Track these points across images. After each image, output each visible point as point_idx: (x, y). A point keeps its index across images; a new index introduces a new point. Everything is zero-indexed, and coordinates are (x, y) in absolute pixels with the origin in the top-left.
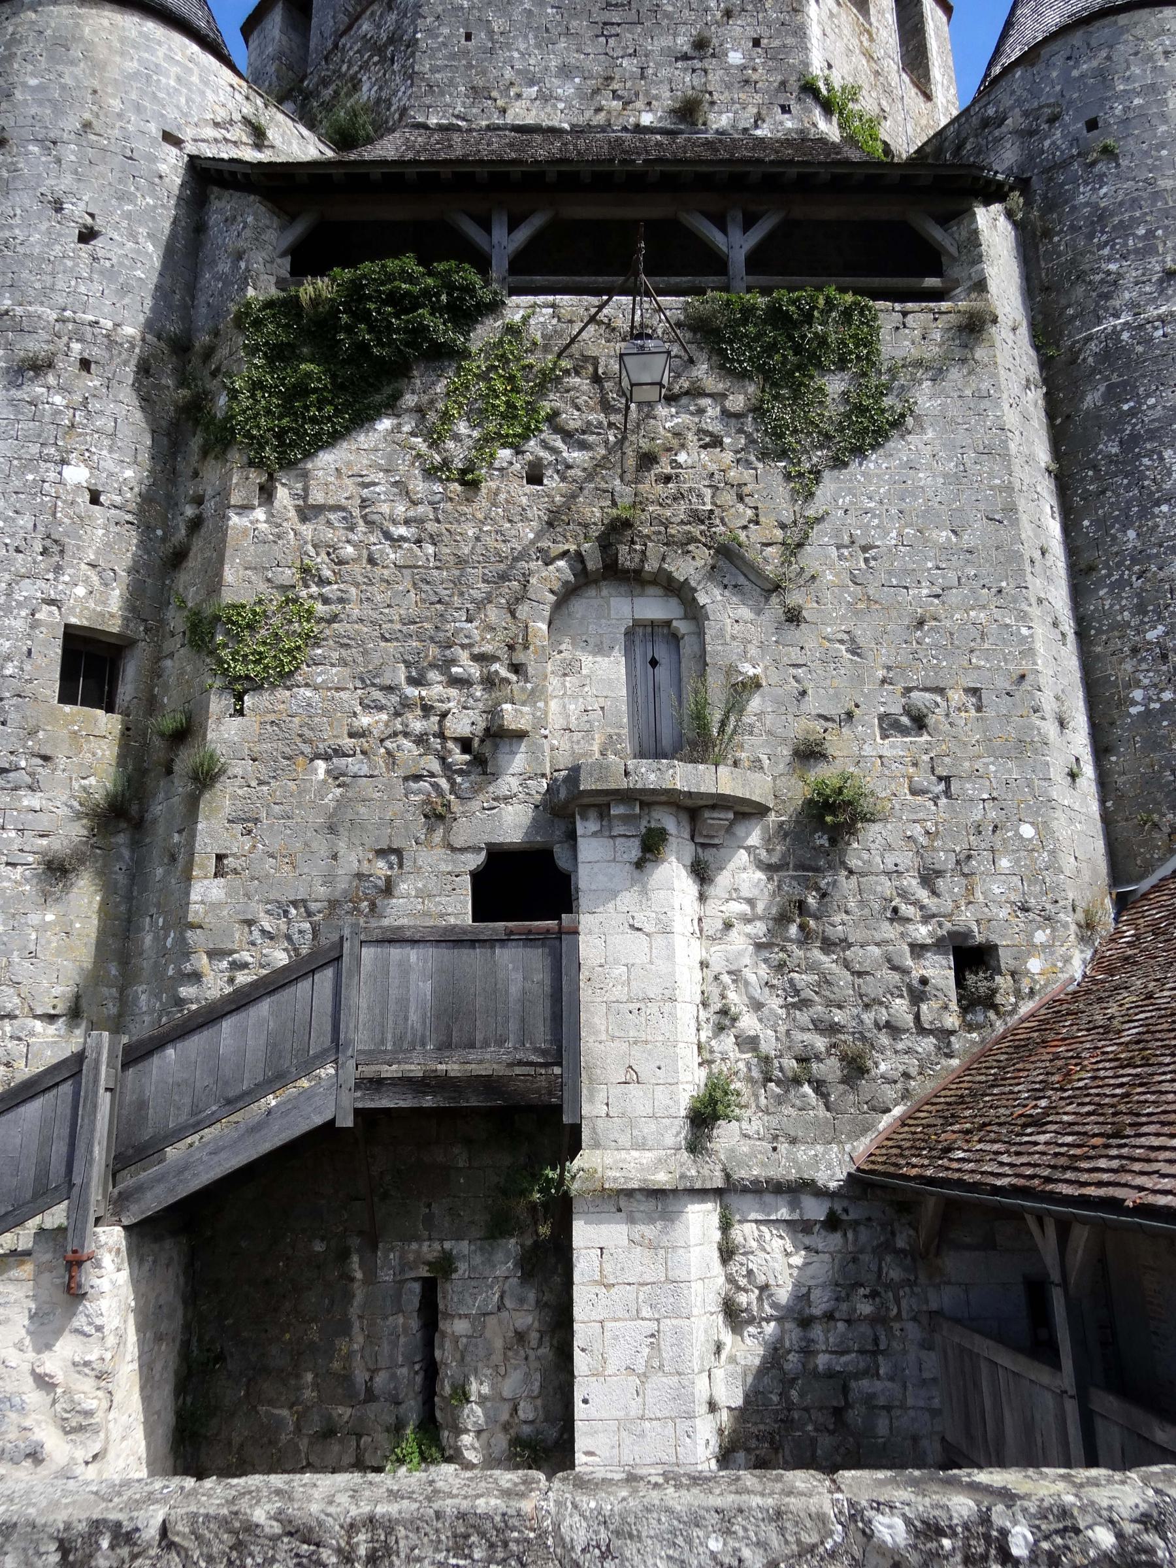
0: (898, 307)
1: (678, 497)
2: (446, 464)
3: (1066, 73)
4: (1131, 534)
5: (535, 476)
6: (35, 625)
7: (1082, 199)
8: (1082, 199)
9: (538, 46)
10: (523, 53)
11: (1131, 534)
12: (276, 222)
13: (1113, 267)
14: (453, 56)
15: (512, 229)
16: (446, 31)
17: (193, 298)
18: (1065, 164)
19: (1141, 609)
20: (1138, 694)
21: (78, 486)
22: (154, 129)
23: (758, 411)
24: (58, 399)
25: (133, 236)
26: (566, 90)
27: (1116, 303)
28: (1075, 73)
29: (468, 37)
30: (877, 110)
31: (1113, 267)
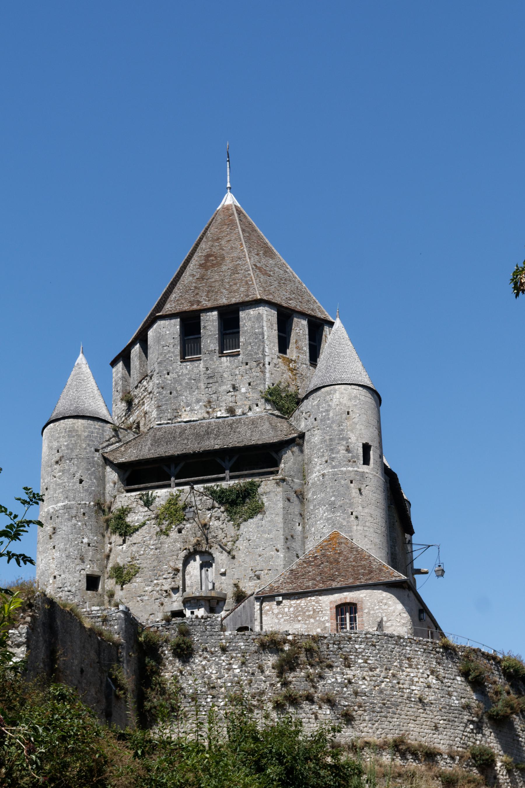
9: (189, 394)
14: (167, 400)
15: (176, 467)
16: (165, 392)
17: (105, 490)
22: (93, 449)
27: (316, 470)
29: (171, 393)
31: (316, 460)
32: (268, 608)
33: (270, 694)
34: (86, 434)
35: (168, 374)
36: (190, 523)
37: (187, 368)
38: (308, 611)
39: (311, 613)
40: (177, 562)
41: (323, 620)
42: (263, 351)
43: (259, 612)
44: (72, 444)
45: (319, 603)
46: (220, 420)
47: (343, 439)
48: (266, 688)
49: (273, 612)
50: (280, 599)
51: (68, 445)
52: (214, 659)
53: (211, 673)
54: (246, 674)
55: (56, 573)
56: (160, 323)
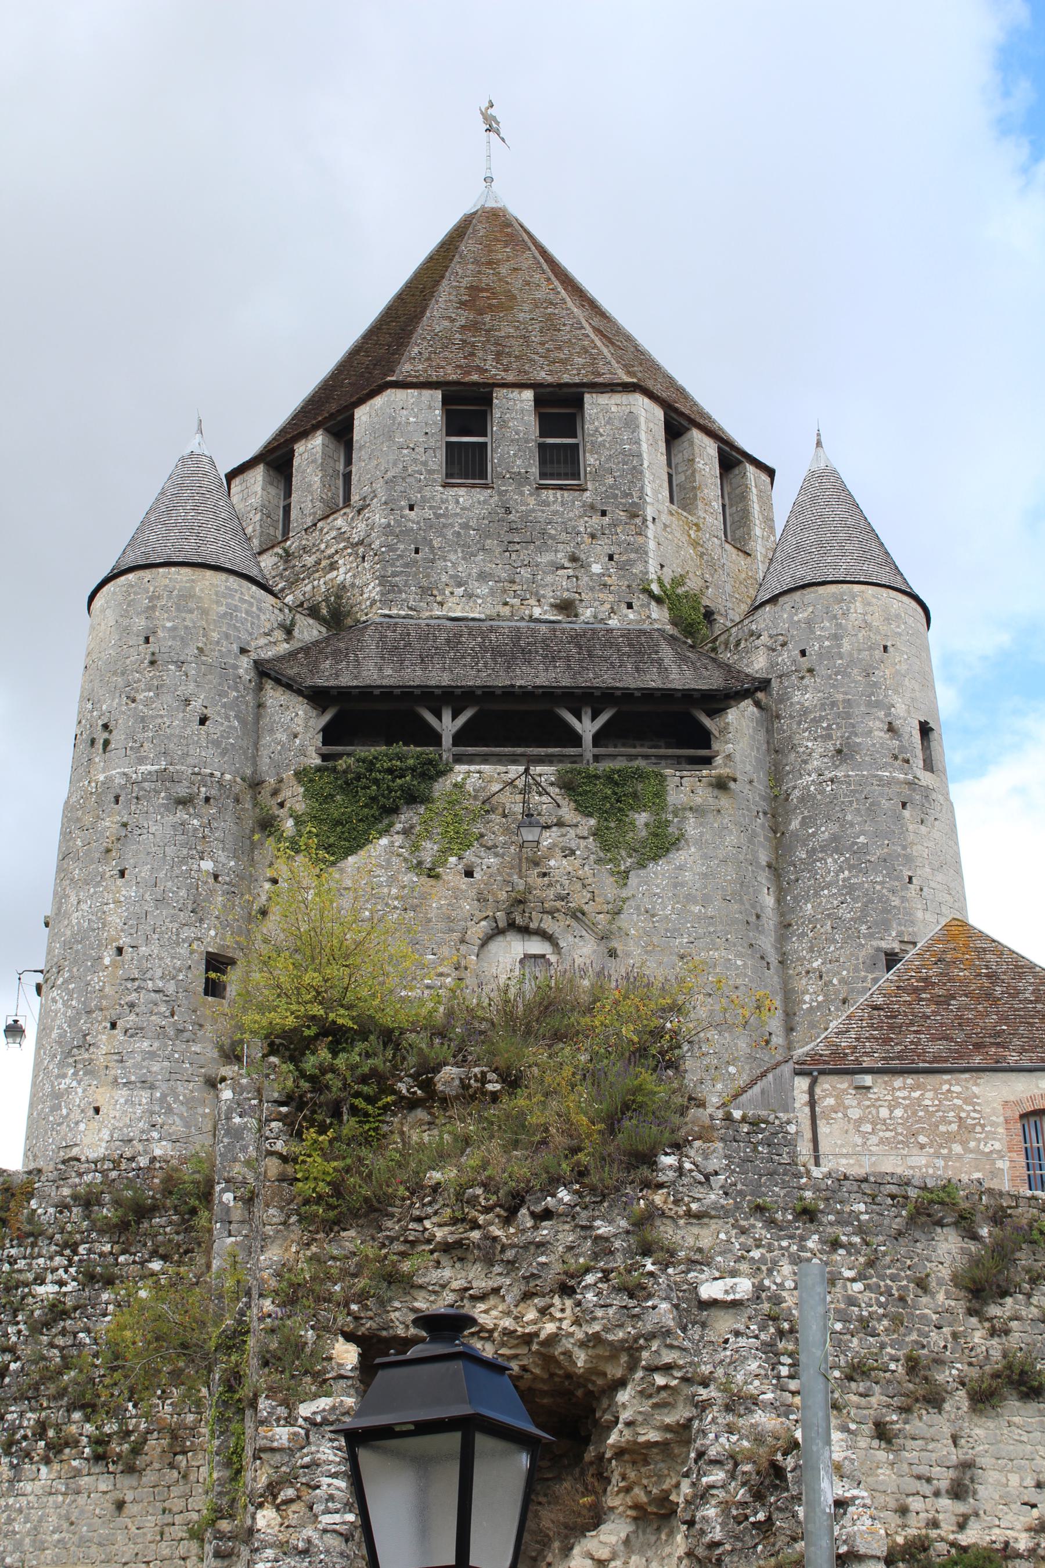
0: (678, 773)
1: (550, 885)
2: (420, 863)
3: (791, 617)
4: (809, 906)
5: (469, 874)
6: (192, 952)
7: (796, 699)
8: (796, 699)
9: (464, 559)
10: (454, 562)
11: (809, 906)
12: (314, 713)
13: (810, 744)
14: (406, 565)
15: (454, 719)
16: (402, 547)
18: (787, 675)
19: (811, 950)
20: (807, 998)
21: (207, 872)
22: (235, 648)
23: (595, 833)
24: (195, 822)
25: (227, 718)
26: (483, 590)
27: (809, 767)
28: (796, 618)
29: (417, 551)
30: (701, 583)
31: (810, 744)
32: (831, 1101)
33: (959, 1366)
34: (222, 609)
35: (411, 508)
36: (496, 855)
37: (457, 502)
38: (944, 1120)
39: (954, 1127)
40: (463, 948)
41: (987, 1150)
42: (642, 489)
43: (807, 1110)
44: (186, 627)
45: (974, 1104)
46: (543, 628)
47: (878, 704)
48: (945, 1347)
49: (845, 1115)
50: (868, 1080)
51: (174, 629)
52: (784, 1243)
53: (781, 1286)
54: (883, 1299)
55: (124, 941)
56: (390, 394)
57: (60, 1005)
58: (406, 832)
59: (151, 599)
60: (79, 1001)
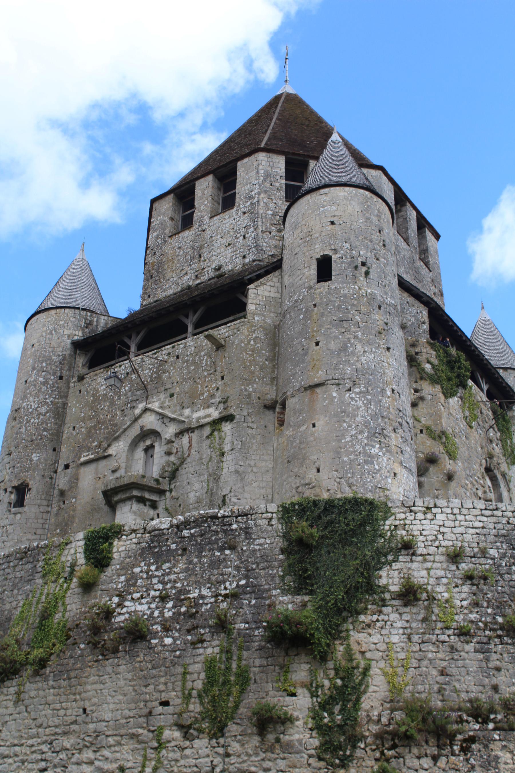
57: (360, 403)
58: (461, 398)
59: (379, 212)
60: (376, 408)
